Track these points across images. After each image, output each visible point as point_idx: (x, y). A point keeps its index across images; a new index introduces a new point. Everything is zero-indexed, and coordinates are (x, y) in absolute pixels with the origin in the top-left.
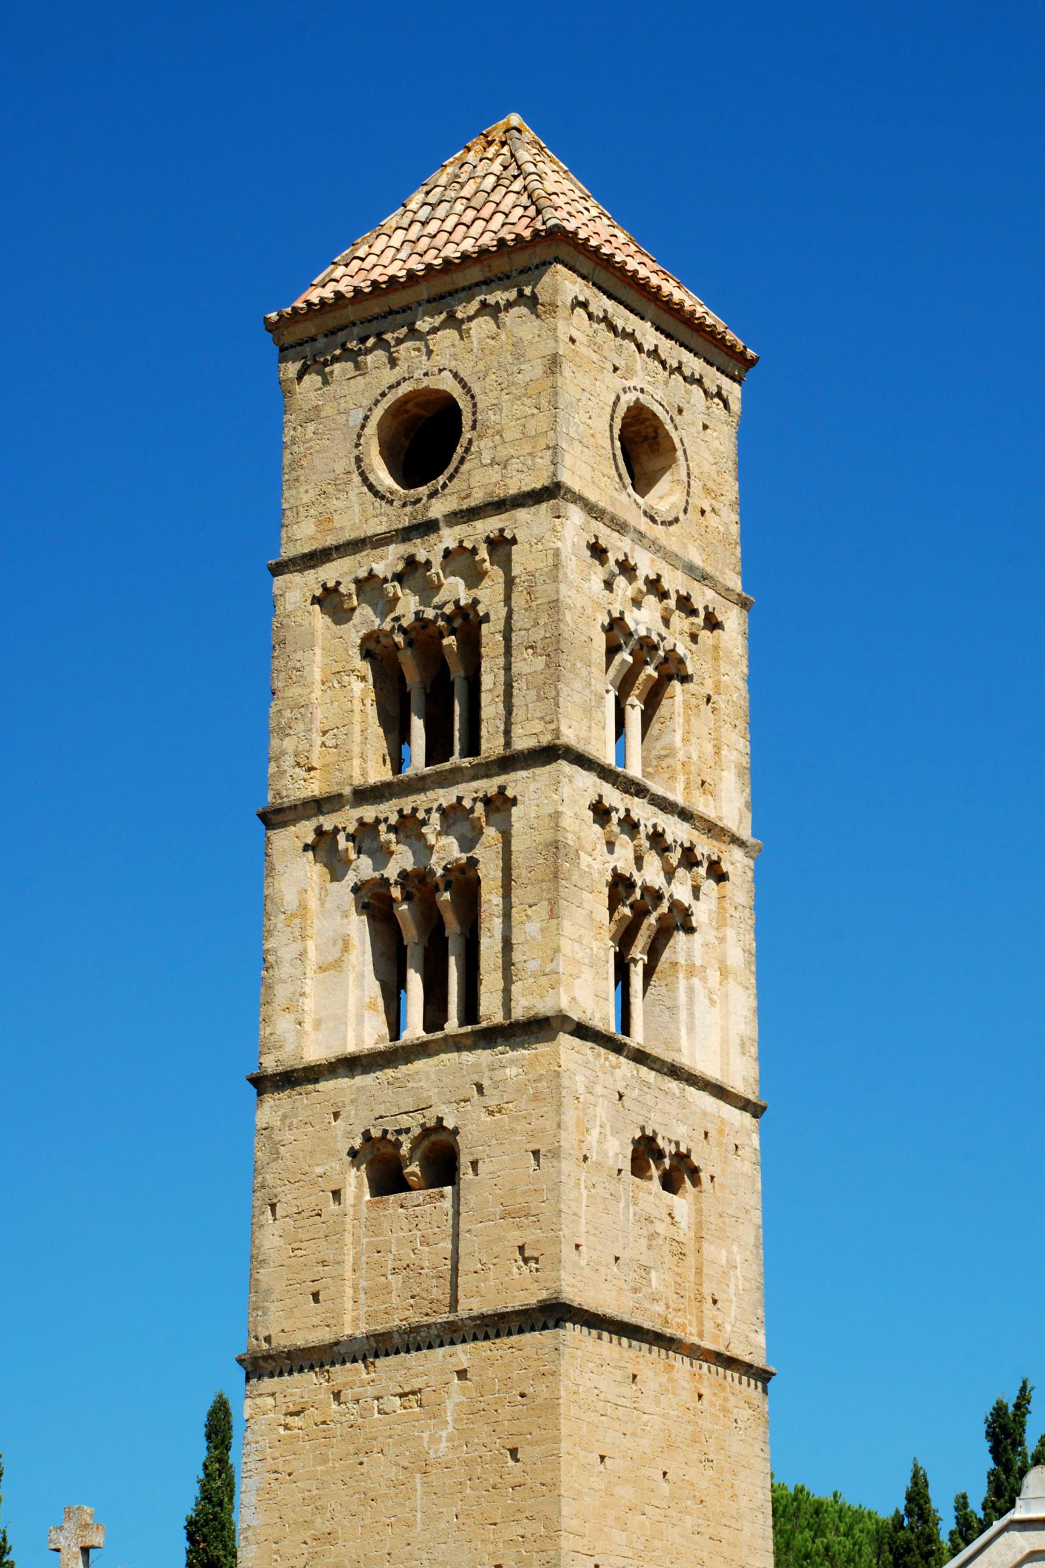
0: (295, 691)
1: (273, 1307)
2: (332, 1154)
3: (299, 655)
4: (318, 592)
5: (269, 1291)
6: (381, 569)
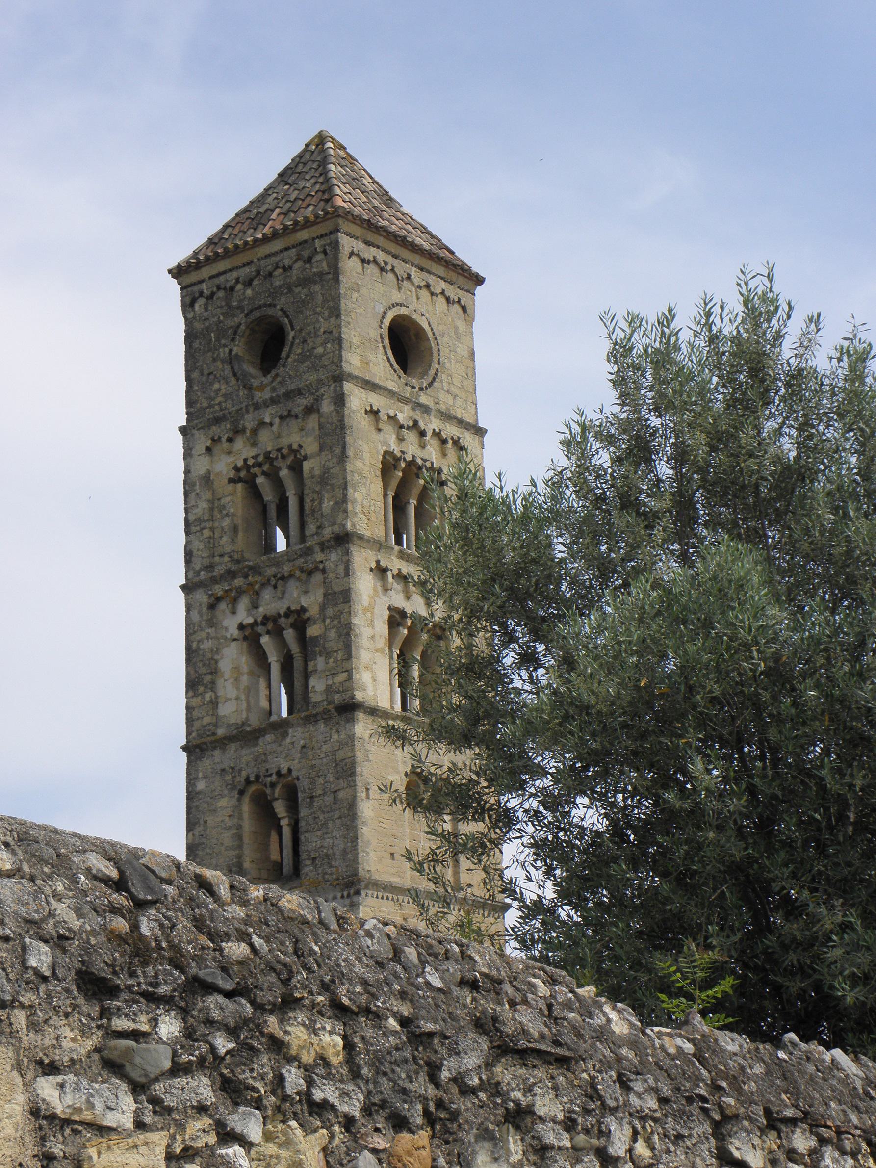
0: (359, 464)
1: (372, 854)
2: (398, 772)
3: (360, 442)
4: (368, 409)
5: (369, 843)
6: (401, 417)
